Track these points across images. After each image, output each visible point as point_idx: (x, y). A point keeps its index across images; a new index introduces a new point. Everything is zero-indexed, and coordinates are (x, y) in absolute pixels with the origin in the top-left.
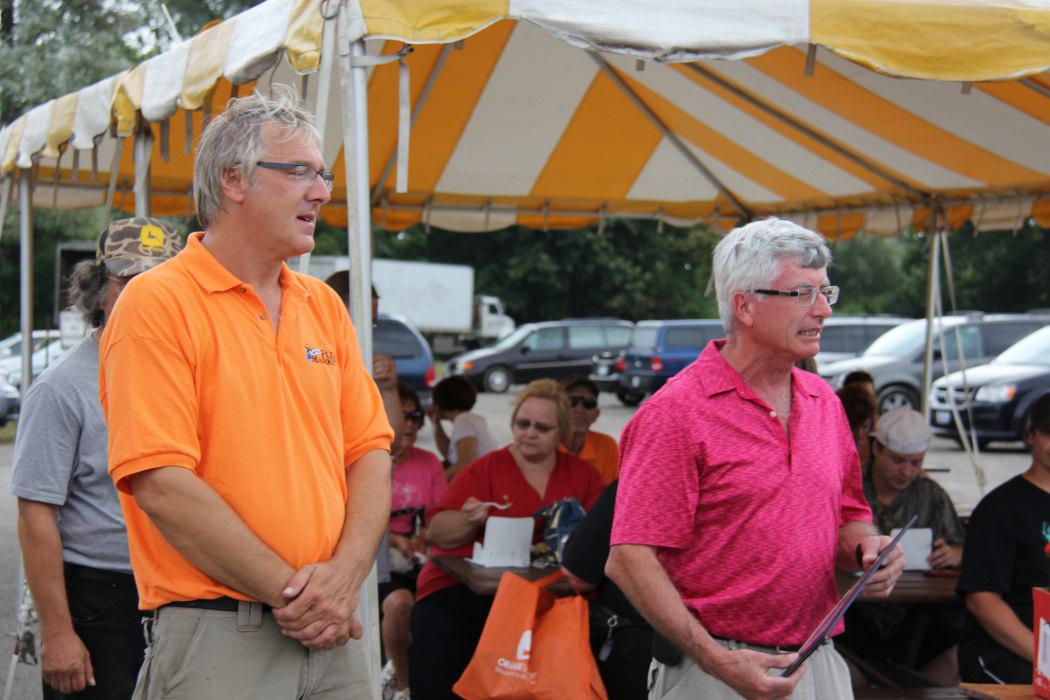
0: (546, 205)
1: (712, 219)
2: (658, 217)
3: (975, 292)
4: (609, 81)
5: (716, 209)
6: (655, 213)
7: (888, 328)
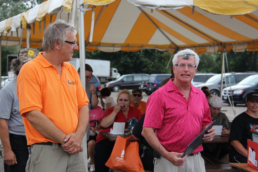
0: (128, 46)
1: (169, 49)
2: (156, 49)
3: (233, 67)
5: (170, 47)
6: (155, 48)
7: (212, 76)
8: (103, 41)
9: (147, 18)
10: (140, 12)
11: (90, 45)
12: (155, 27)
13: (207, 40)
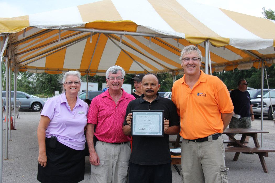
2: (135, 74)
4: (122, 51)
8: (99, 68)
9: (125, 54)
10: (121, 50)
11: (91, 72)
12: (132, 60)
13: (164, 68)
